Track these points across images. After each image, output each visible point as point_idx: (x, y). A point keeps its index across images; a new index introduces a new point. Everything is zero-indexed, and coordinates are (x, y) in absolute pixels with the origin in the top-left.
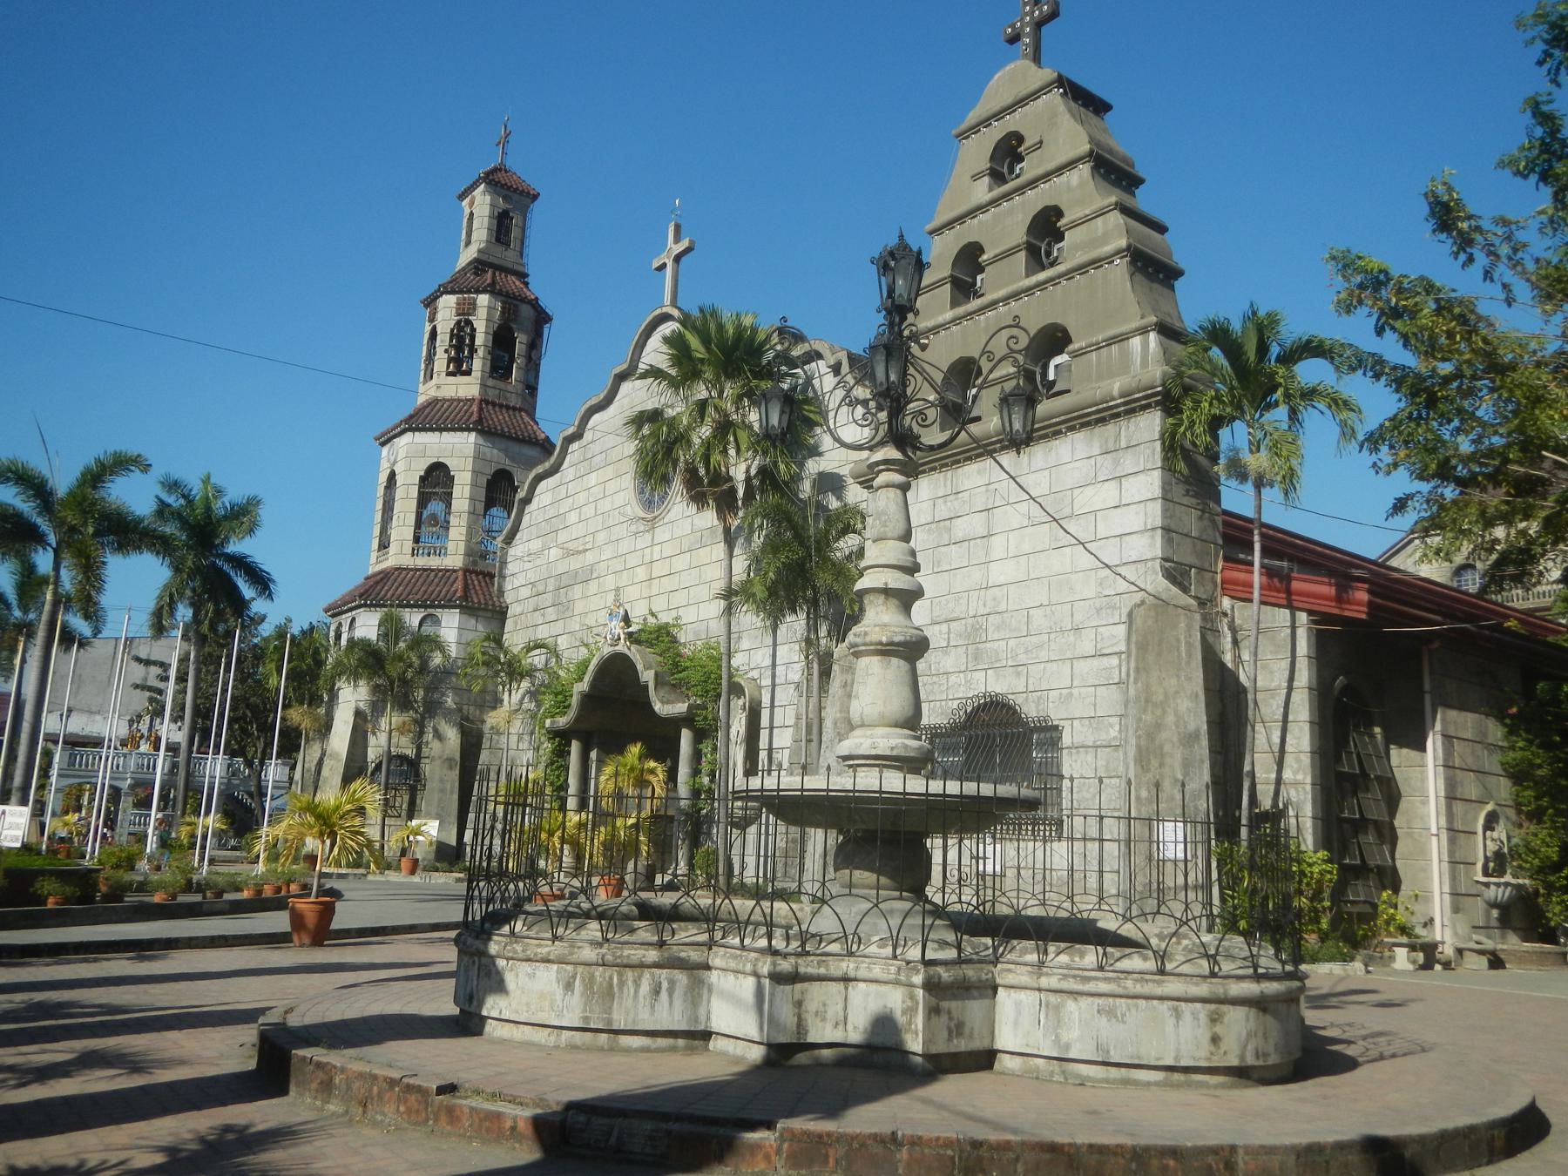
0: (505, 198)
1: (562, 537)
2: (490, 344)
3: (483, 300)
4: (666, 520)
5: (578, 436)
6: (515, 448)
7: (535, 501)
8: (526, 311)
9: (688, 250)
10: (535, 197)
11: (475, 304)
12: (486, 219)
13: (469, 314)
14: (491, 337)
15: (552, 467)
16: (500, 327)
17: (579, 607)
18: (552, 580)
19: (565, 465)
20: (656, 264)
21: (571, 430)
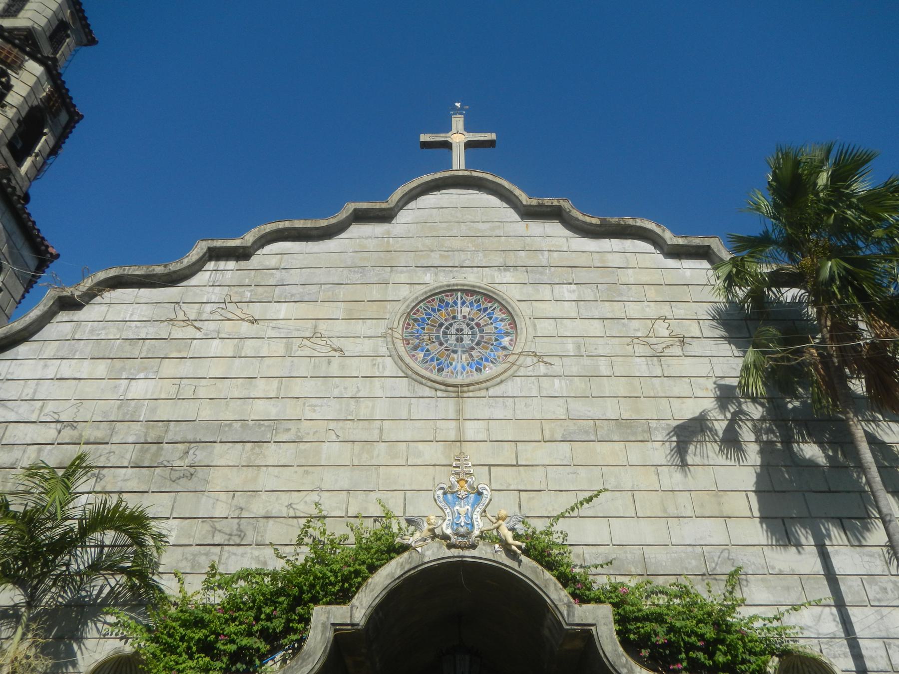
0: (72, 13)
1: (169, 368)
2: (23, 114)
3: (34, 68)
4: (491, 392)
5: (242, 254)
6: (19, 241)
7: (91, 312)
8: (64, 117)
9: (491, 143)
10: (92, 42)
11: (22, 62)
12: (49, 13)
13: (9, 66)
14: (27, 109)
15: (169, 274)
16: (37, 107)
17: (218, 479)
18: (136, 427)
19: (194, 281)
20: (424, 138)
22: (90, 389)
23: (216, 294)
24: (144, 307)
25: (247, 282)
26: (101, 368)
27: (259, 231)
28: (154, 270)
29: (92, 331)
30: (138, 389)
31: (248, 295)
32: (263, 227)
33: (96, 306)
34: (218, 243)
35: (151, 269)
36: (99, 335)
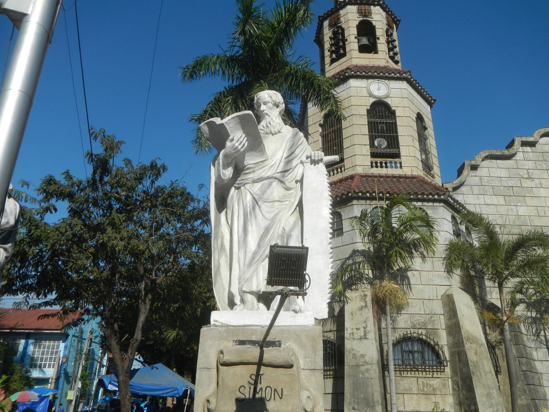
5: (532, 144)
21: (531, 139)
22: (503, 210)
23: (530, 165)
24: (504, 170)
25: (540, 159)
26: (501, 200)
27: (538, 132)
28: (504, 153)
29: (488, 181)
30: (522, 211)
31: (545, 167)
32: (539, 130)
33: (483, 169)
34: (524, 139)
35: (503, 152)
36: (492, 184)
